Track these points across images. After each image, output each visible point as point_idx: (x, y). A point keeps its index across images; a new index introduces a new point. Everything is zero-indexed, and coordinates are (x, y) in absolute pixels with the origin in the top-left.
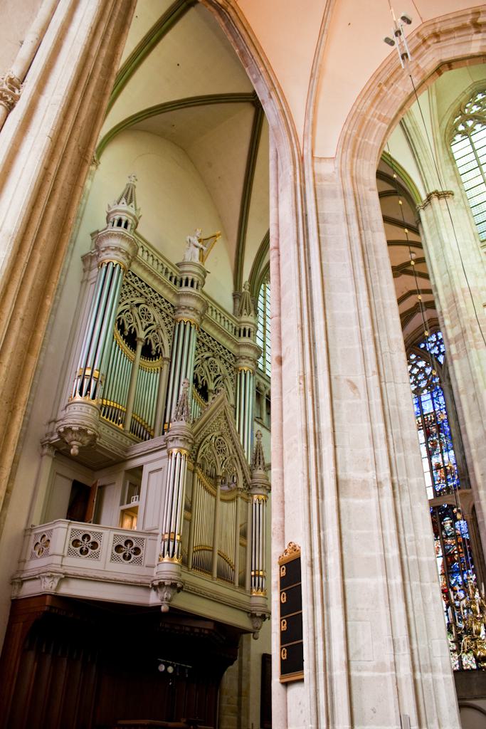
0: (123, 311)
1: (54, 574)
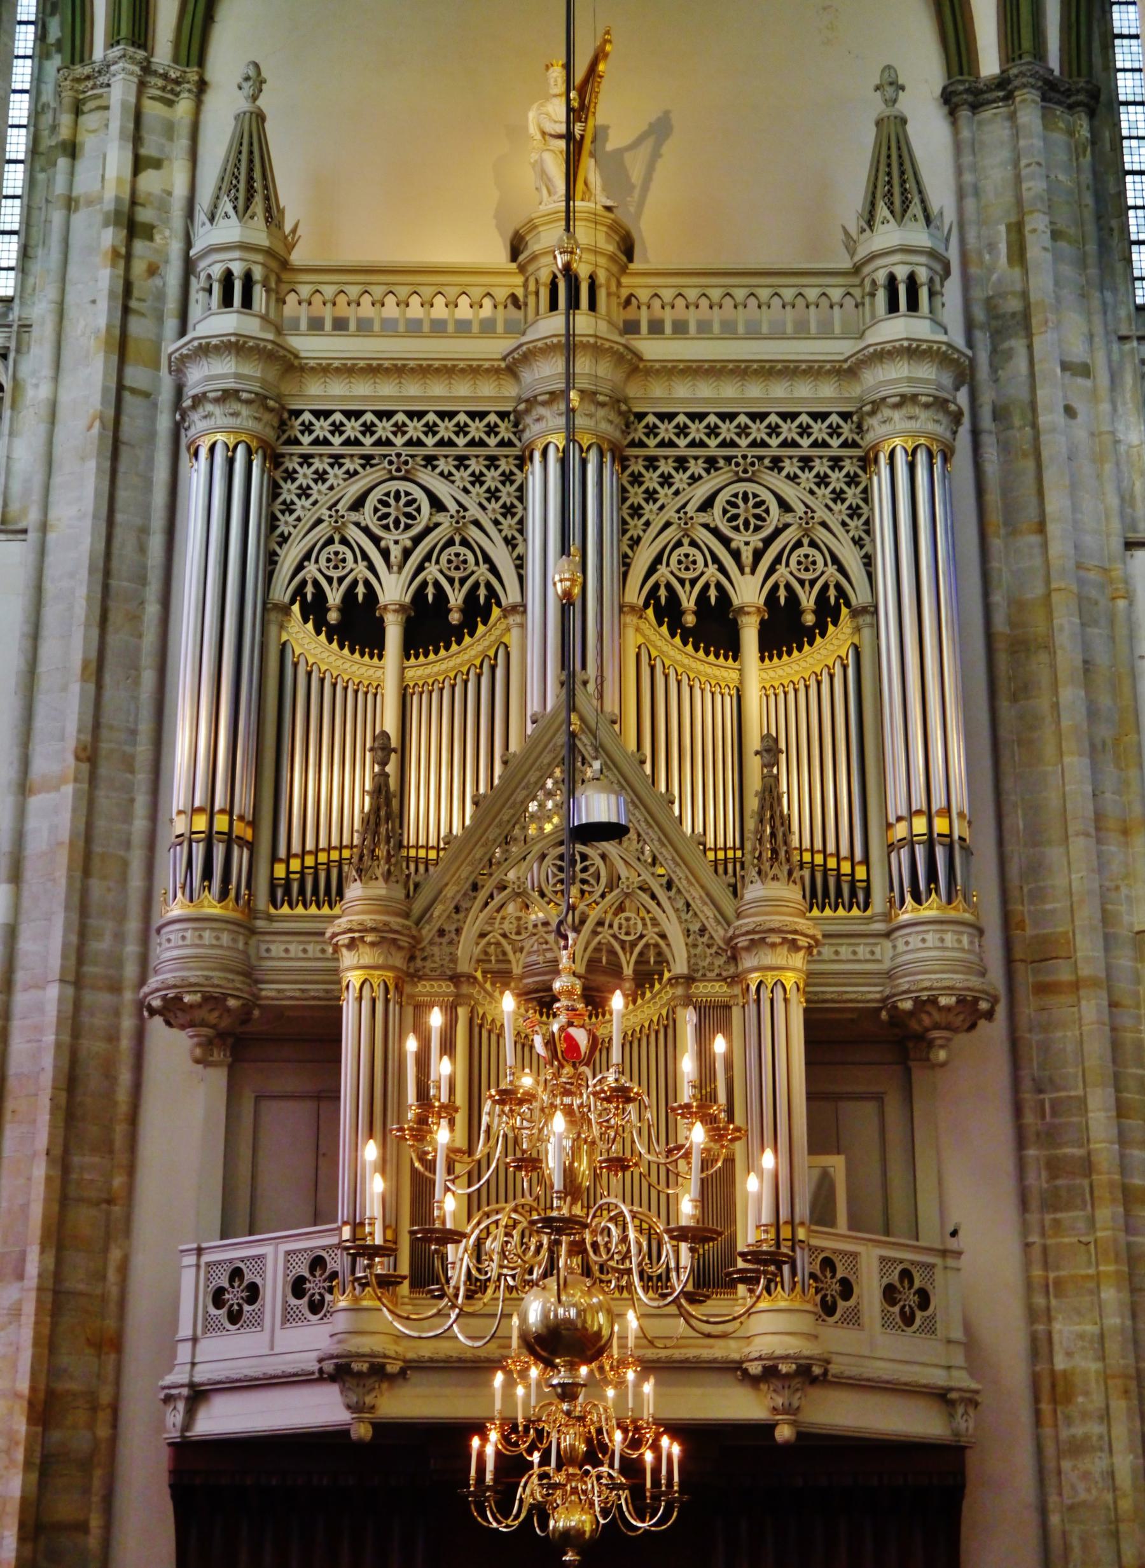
0: (307, 557)
1: (174, 1392)
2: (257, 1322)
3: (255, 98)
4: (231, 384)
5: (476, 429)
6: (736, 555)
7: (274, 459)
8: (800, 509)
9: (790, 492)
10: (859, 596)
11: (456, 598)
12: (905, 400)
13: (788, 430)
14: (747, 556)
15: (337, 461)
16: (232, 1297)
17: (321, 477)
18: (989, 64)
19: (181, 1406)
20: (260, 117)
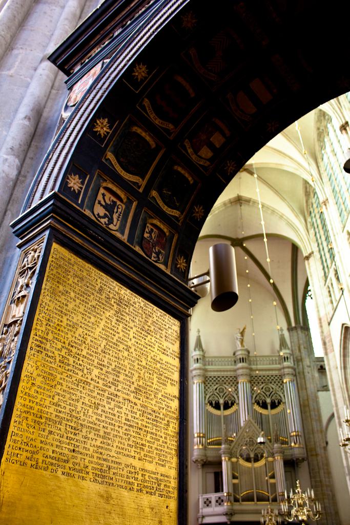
2: (211, 506)
3: (199, 333)
4: (199, 374)
5: (231, 379)
6: (267, 395)
7: (205, 383)
8: (274, 389)
9: (273, 386)
10: (283, 401)
11: (230, 402)
12: (288, 374)
13: (272, 378)
14: (268, 395)
15: (213, 383)
16: (208, 502)
17: (211, 386)
18: (293, 325)
19: (201, 519)
20: (200, 336)
